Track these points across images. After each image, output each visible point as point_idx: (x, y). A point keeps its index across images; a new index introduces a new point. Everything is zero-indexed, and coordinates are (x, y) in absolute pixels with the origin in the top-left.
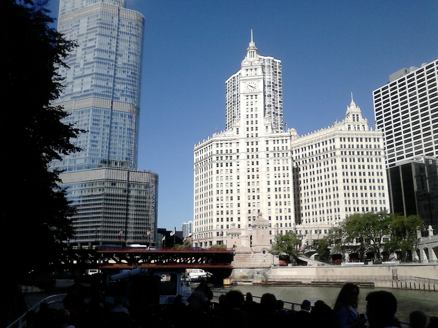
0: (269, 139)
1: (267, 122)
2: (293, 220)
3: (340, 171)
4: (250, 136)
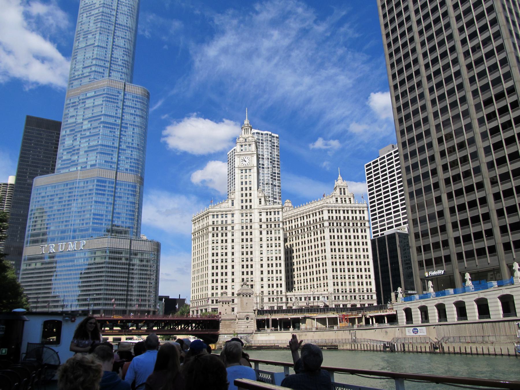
0: (262, 211)
1: (260, 195)
2: (284, 289)
3: (328, 241)
4: (244, 208)
